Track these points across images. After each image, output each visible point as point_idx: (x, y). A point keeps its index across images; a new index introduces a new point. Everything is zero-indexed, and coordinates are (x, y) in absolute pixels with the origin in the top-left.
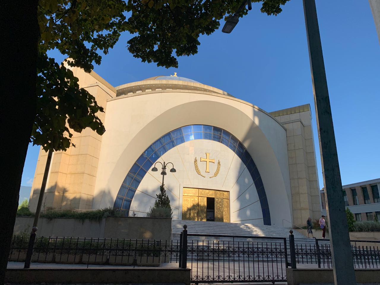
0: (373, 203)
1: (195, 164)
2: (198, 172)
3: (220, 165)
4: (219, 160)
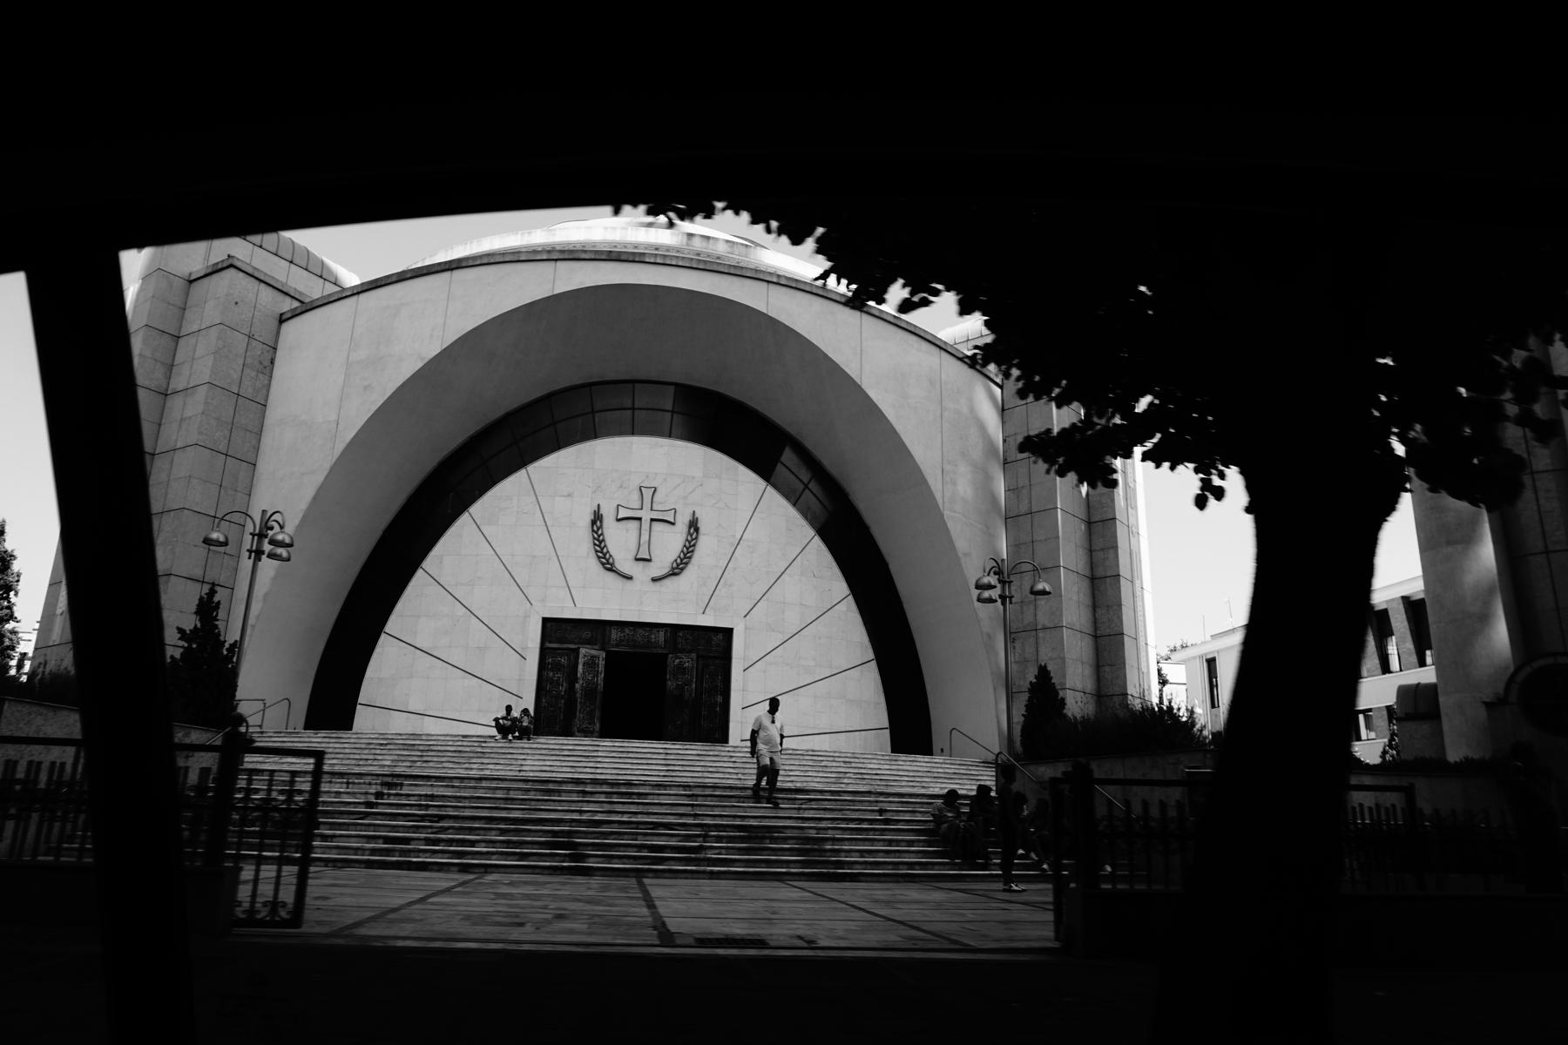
0: (1415, 668)
1: (593, 531)
2: (608, 564)
3: (697, 530)
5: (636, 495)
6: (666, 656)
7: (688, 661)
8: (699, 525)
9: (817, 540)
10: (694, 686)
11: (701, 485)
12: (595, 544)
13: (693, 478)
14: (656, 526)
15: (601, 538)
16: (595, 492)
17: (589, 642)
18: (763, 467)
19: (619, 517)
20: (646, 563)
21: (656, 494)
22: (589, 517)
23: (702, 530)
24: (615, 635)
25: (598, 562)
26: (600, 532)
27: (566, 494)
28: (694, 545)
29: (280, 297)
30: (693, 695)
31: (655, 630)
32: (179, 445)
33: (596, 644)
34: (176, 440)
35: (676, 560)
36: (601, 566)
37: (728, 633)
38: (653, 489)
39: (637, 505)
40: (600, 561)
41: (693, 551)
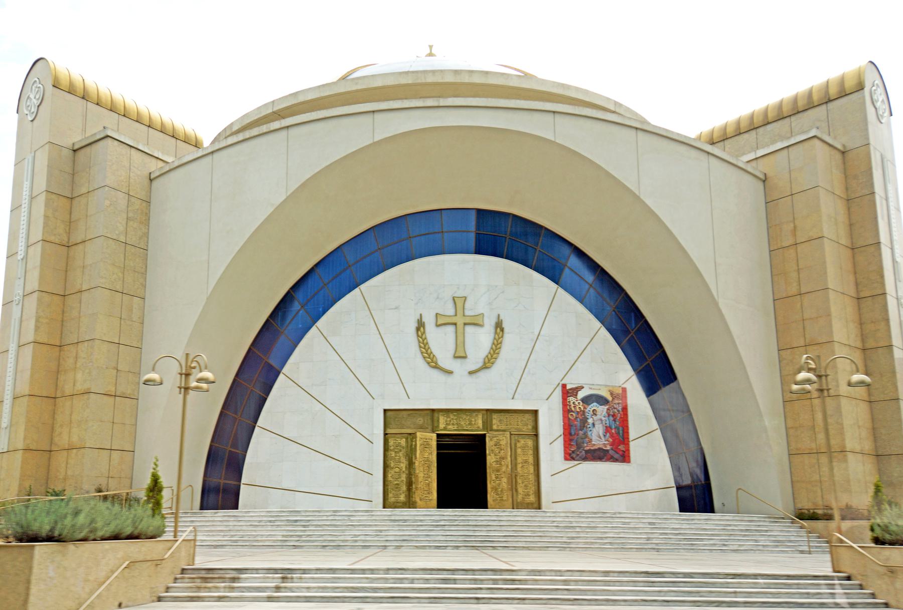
1: (418, 336)
3: (502, 330)
4: (499, 315)
5: (450, 305)
6: (484, 435)
7: (504, 440)
8: (503, 326)
9: (604, 332)
10: (509, 459)
11: (503, 292)
12: (420, 347)
13: (496, 286)
14: (469, 329)
15: (425, 341)
16: (417, 304)
17: (422, 428)
18: (553, 273)
19: (438, 324)
20: (463, 360)
21: (466, 302)
22: (414, 325)
23: (506, 330)
24: (442, 421)
25: (424, 360)
26: (424, 337)
27: (394, 307)
28: (501, 343)
29: (148, 159)
30: (510, 467)
31: (474, 414)
32: (84, 288)
33: (427, 428)
34: (81, 285)
35: (487, 356)
36: (426, 364)
37: (536, 412)
38: (464, 298)
39: (451, 312)
40: (426, 361)
41: (500, 348)
